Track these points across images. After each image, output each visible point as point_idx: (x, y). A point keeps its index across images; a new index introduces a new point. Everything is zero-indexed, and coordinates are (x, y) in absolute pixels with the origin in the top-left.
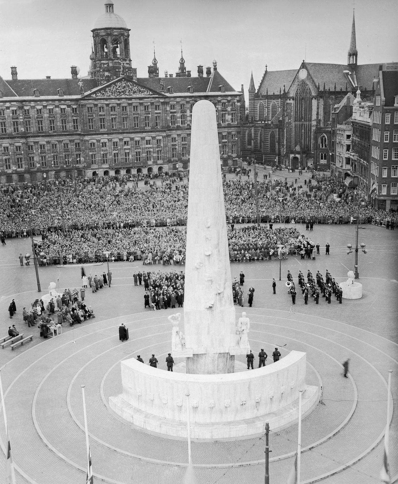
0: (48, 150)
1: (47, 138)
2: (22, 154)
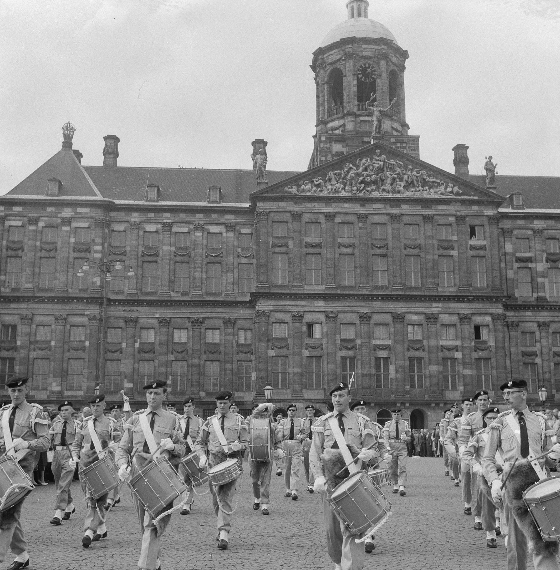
0: (161, 344)
1: (161, 309)
2: (83, 349)
